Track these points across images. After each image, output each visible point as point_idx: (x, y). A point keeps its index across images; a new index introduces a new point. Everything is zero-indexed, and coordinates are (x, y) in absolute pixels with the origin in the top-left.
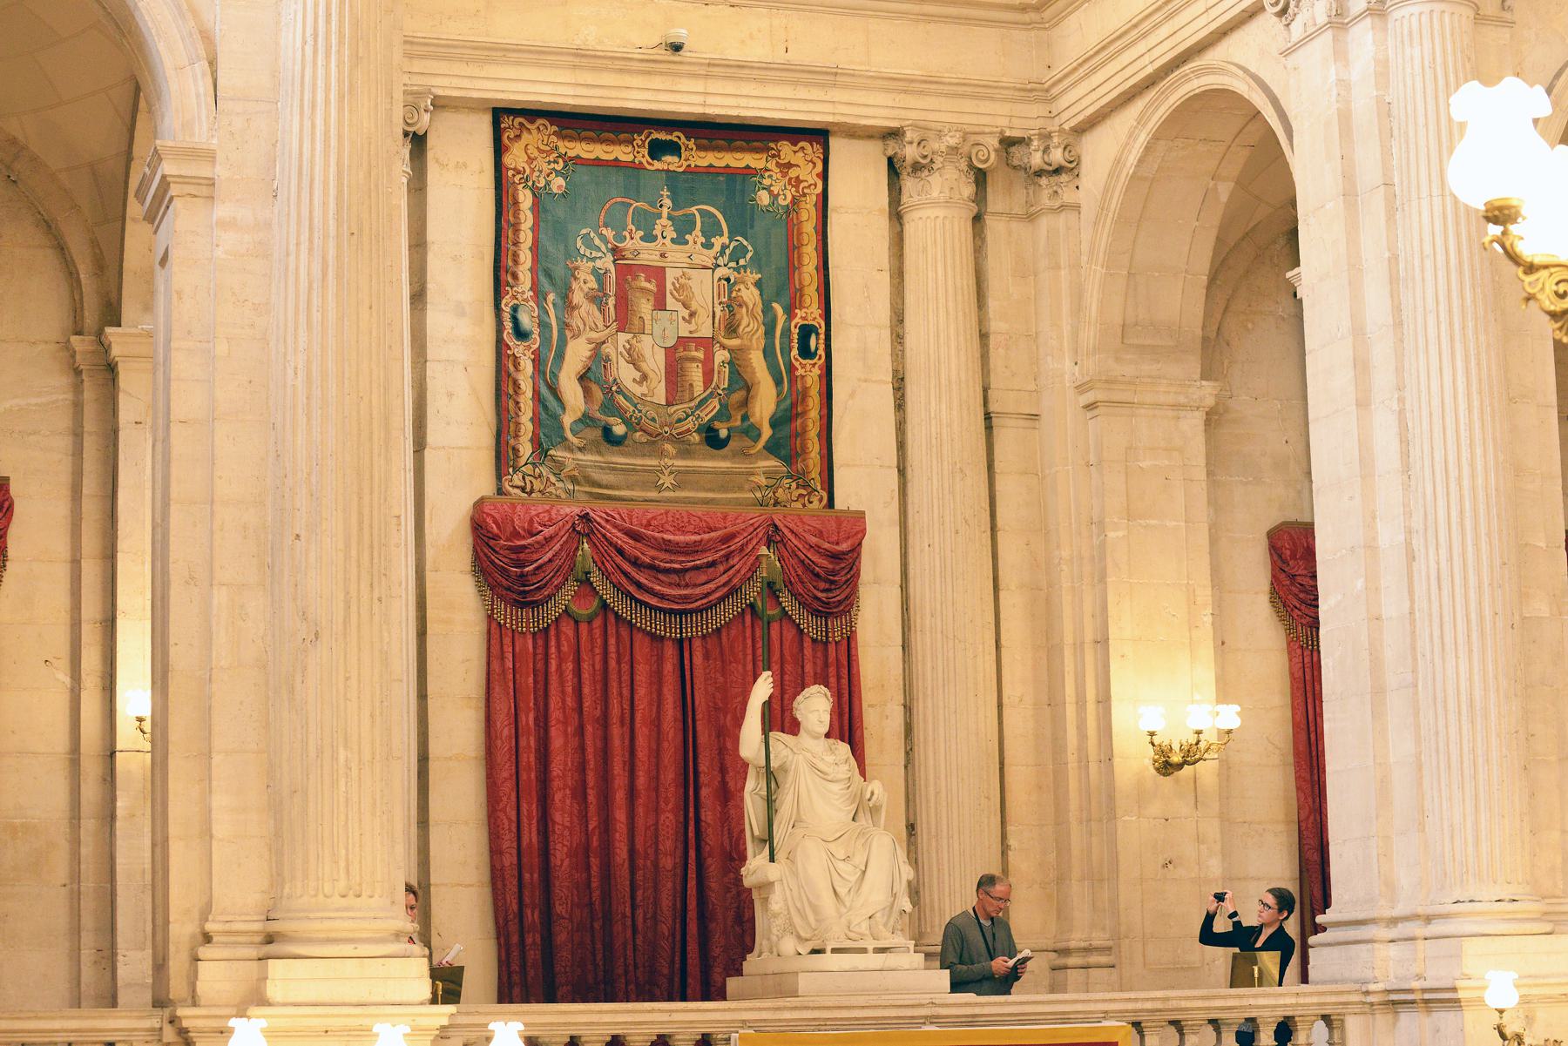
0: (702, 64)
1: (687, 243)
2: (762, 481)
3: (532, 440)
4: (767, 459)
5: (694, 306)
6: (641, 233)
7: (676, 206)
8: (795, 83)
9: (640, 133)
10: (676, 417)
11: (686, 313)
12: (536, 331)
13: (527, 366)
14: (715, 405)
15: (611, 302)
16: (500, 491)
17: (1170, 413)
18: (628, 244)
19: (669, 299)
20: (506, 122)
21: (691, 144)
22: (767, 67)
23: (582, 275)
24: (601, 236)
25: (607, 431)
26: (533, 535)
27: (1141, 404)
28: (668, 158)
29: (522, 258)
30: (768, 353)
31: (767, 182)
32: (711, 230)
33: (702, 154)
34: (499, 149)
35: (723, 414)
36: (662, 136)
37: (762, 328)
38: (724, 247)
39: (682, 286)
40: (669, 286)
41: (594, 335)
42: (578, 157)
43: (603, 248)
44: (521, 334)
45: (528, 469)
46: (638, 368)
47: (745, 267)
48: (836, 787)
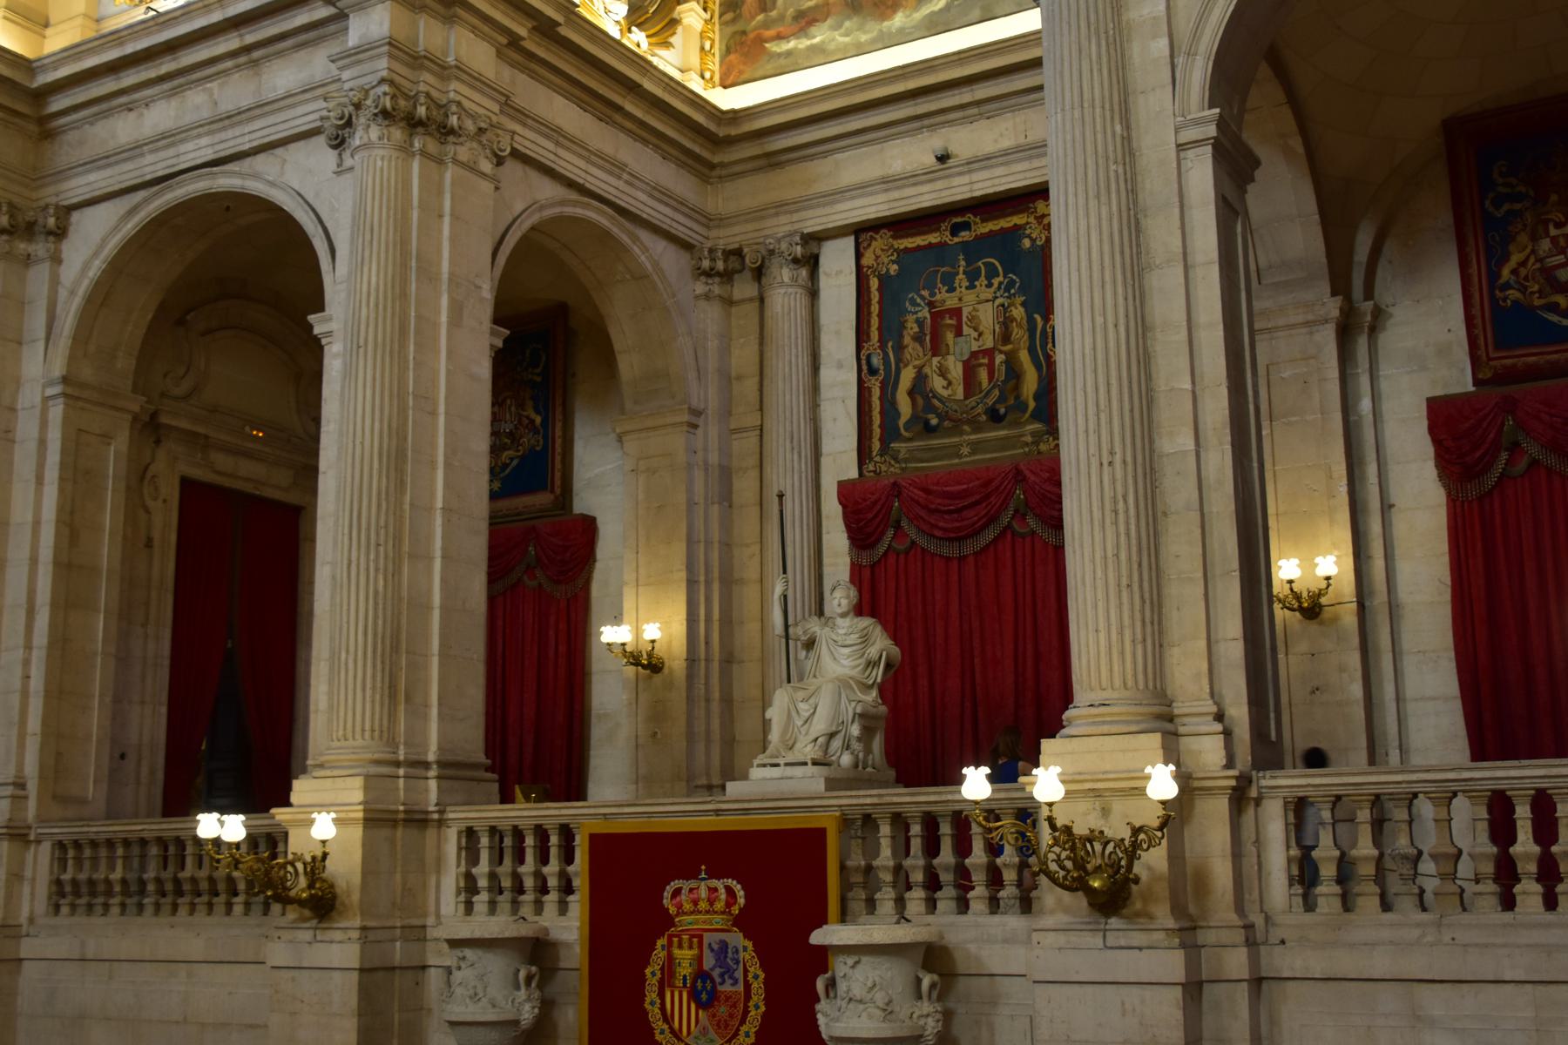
0: (962, 165)
1: (975, 287)
2: (1029, 439)
3: (880, 440)
4: (1032, 423)
5: (981, 328)
6: (946, 288)
7: (968, 264)
8: (1030, 158)
9: (944, 221)
10: (970, 406)
11: (975, 334)
12: (882, 367)
13: (876, 393)
14: (997, 392)
15: (928, 338)
16: (861, 474)
17: (1304, 330)
18: (938, 297)
19: (966, 330)
20: (863, 237)
21: (978, 220)
22: (1006, 153)
23: (909, 325)
24: (923, 298)
25: (927, 423)
26: (865, 500)
27: (1276, 328)
28: (963, 234)
29: (873, 321)
30: (1032, 351)
31: (1028, 232)
32: (992, 272)
33: (985, 224)
34: (859, 256)
35: (1001, 399)
36: (959, 220)
37: (1027, 334)
38: (1000, 283)
39: (973, 317)
40: (964, 319)
41: (917, 362)
42: (906, 248)
43: (922, 304)
44: (873, 371)
45: (878, 459)
46: (945, 378)
47: (1014, 294)
48: (846, 651)
